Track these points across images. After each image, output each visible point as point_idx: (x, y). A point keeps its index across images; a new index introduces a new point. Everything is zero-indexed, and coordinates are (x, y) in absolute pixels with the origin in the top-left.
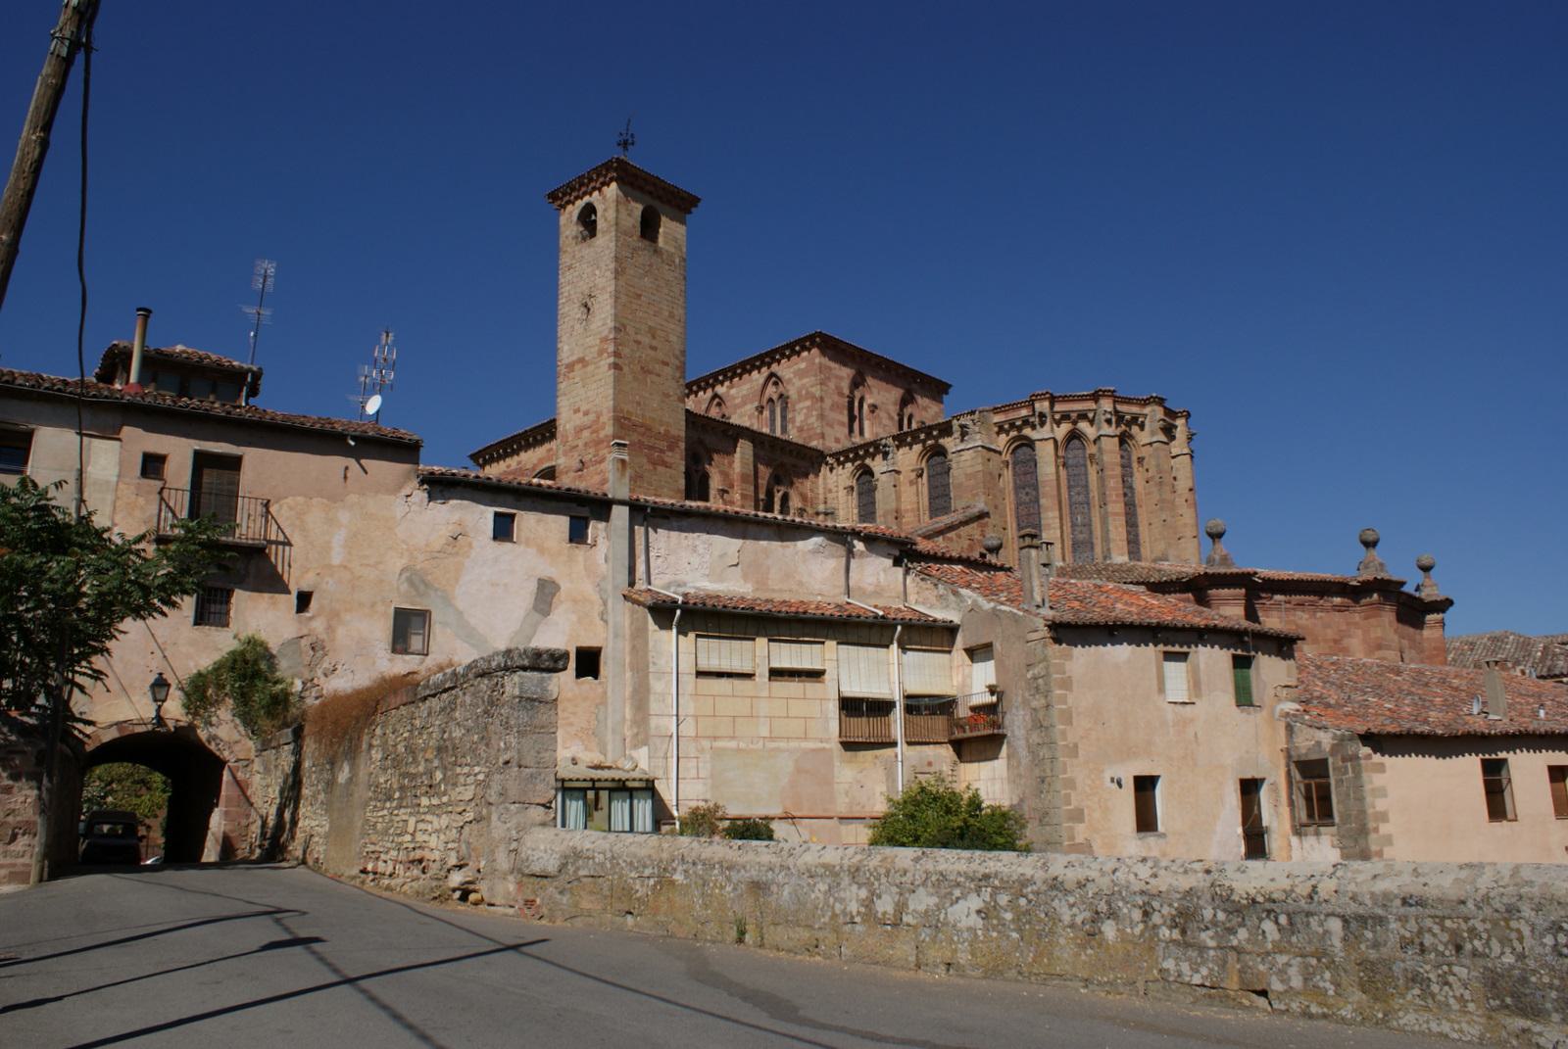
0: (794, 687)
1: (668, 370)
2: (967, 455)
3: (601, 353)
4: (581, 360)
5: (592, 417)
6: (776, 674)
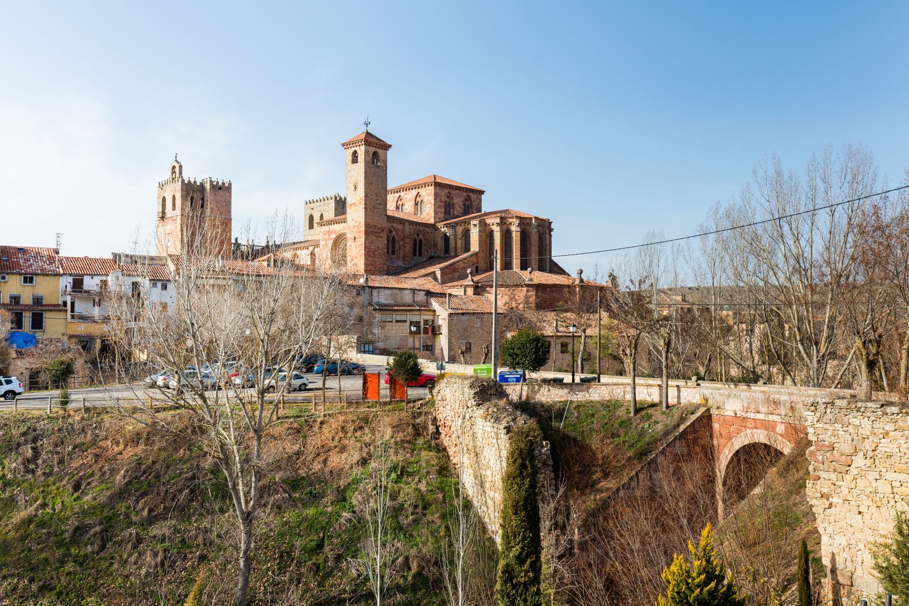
0: (400, 324)
1: (381, 206)
3: (360, 203)
4: (354, 204)
5: (358, 223)
6: (397, 321)
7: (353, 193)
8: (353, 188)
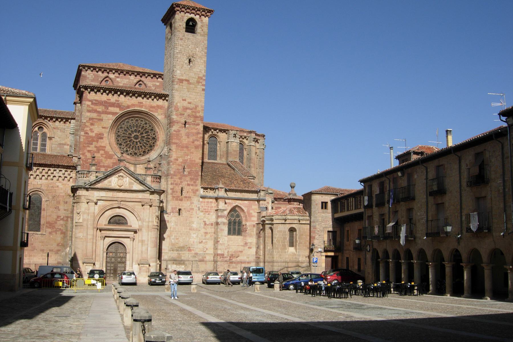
2: (234, 144)
3: (198, 82)
4: (187, 81)
7: (186, 66)
8: (187, 61)
